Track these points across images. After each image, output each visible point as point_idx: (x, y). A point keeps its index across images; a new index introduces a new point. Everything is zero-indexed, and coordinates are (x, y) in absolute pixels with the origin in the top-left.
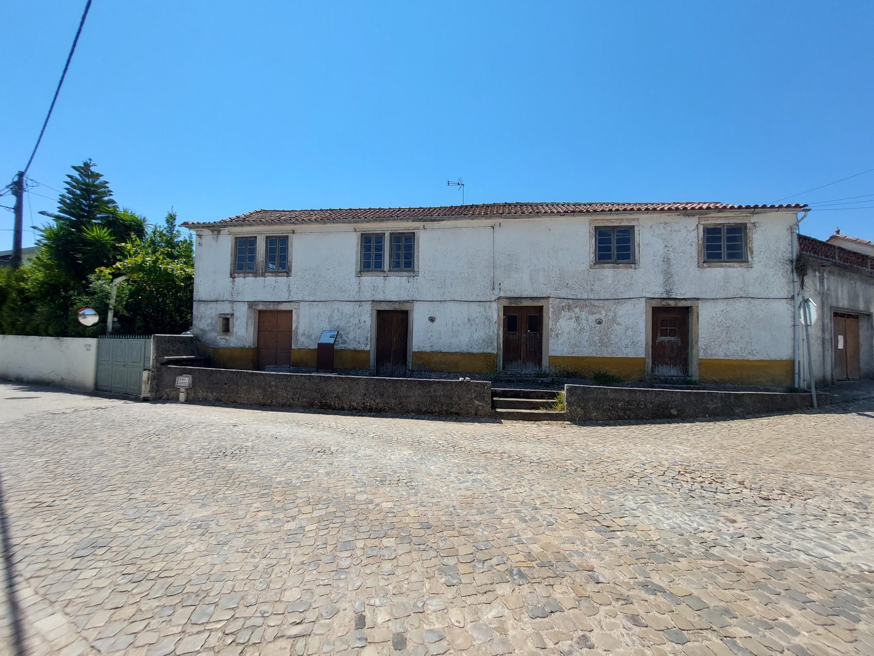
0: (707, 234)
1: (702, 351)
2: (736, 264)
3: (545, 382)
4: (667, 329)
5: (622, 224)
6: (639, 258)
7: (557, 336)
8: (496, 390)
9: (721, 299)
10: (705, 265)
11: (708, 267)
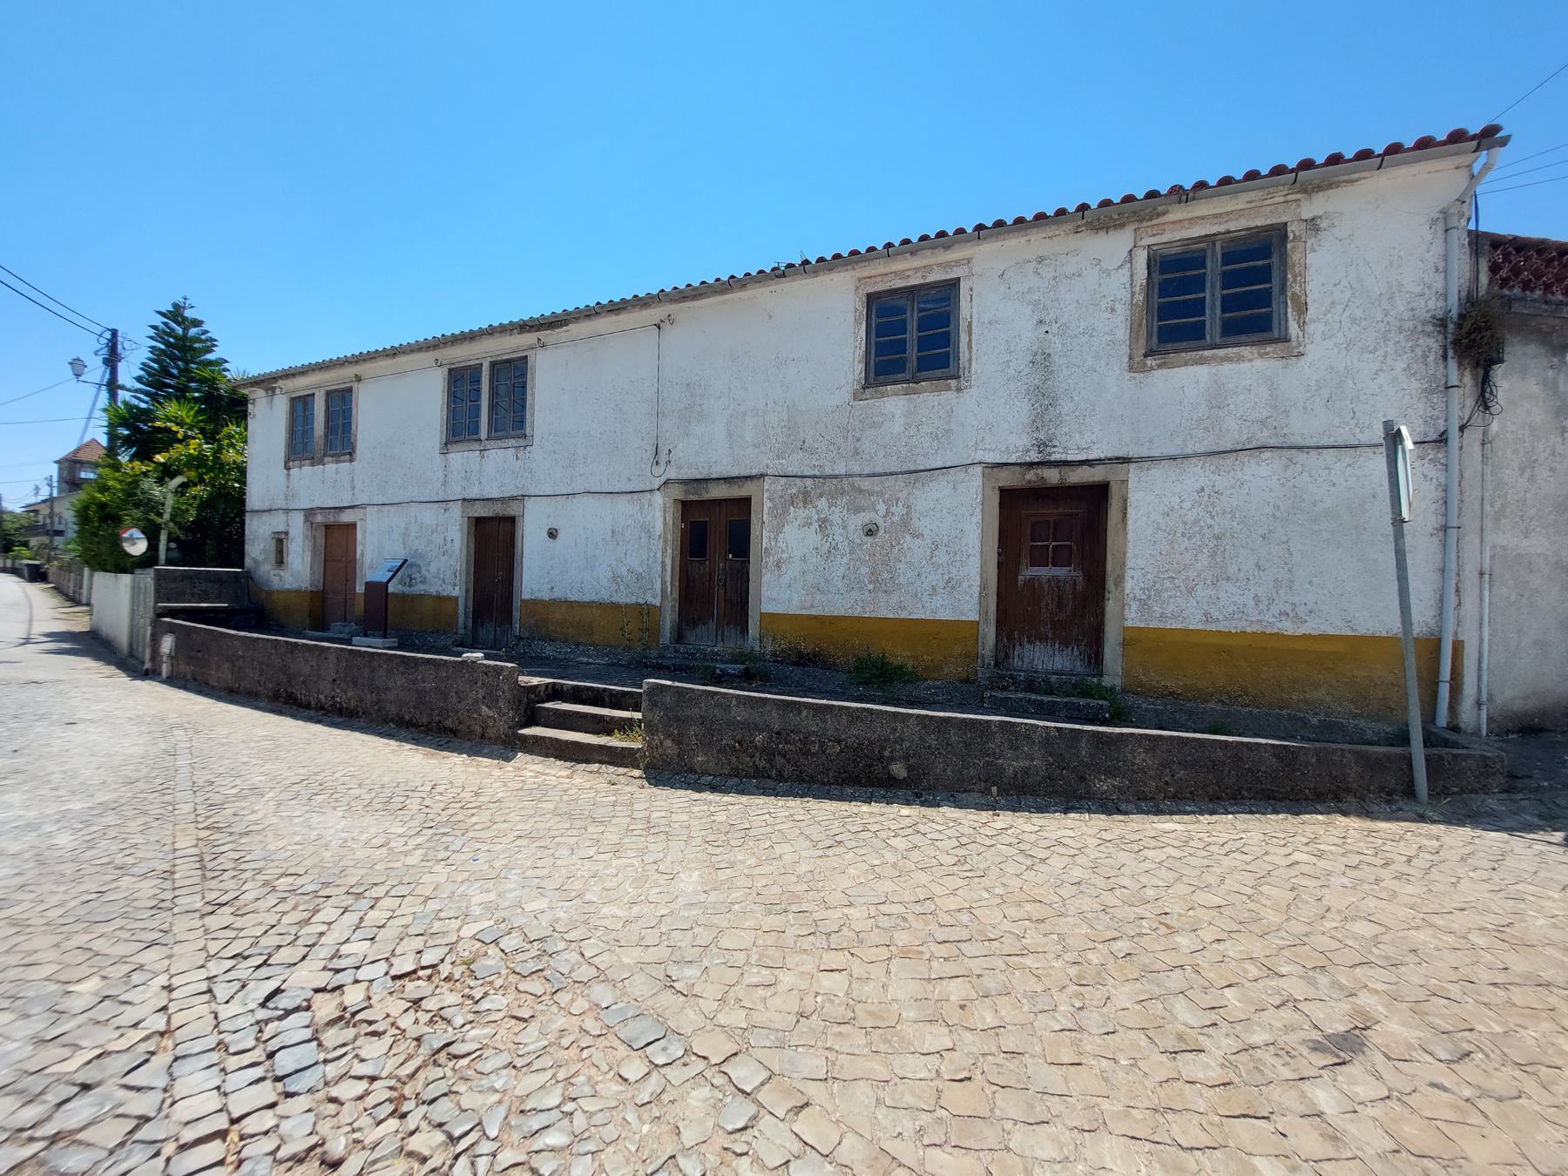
0: (1162, 273)
1: (1134, 606)
2: (1245, 351)
3: (730, 675)
4: (1048, 546)
5: (931, 278)
6: (970, 360)
7: (778, 565)
8: (562, 685)
9: (1196, 455)
10: (1150, 361)
11: (1160, 366)
